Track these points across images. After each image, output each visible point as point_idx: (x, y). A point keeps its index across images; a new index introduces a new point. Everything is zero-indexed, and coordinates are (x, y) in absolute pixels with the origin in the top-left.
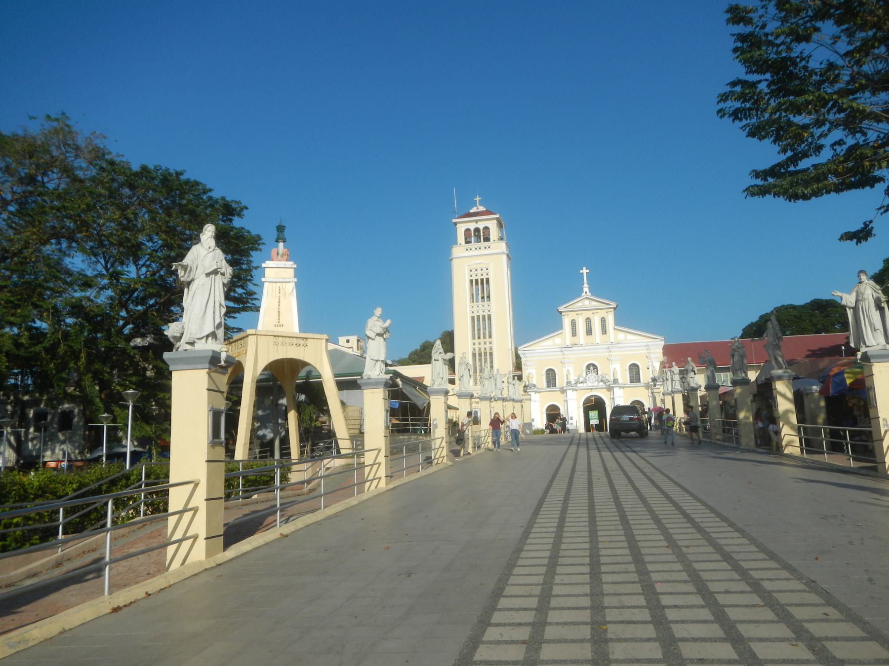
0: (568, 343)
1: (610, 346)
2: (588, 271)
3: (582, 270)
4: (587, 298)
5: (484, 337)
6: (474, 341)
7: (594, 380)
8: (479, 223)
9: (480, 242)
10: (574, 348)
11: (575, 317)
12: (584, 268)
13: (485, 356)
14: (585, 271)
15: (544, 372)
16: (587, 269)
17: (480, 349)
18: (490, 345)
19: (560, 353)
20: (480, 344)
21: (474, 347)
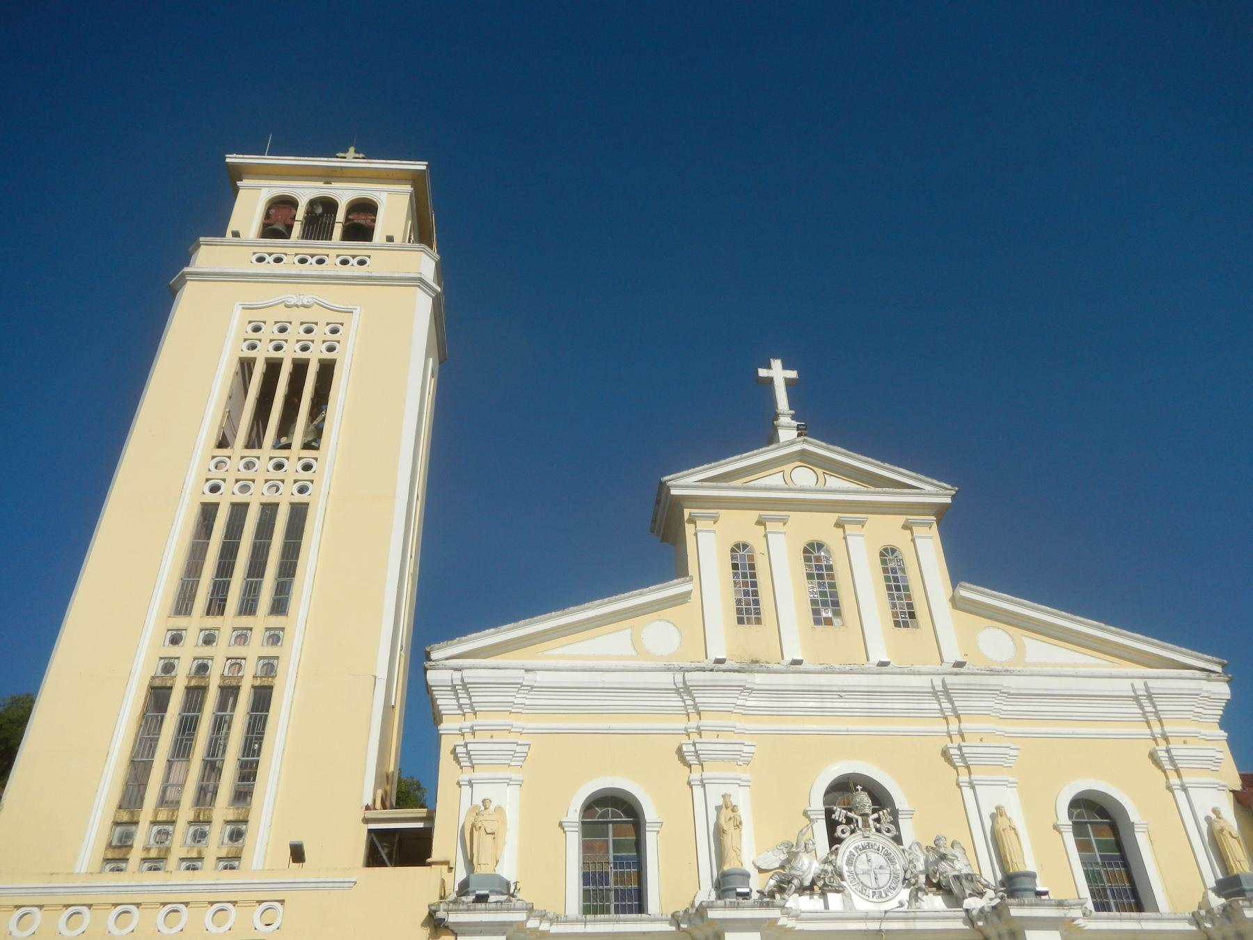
0: (717, 652)
1: (949, 679)
2: (793, 374)
3: (769, 367)
4: (805, 458)
5: (248, 607)
6: (180, 622)
7: (884, 879)
8: (334, 185)
9: (329, 237)
10: (759, 679)
11: (753, 536)
12: (777, 364)
13: (222, 706)
14: (778, 373)
15: (574, 815)
16: (785, 367)
17: (202, 669)
18: (270, 651)
19: (675, 701)
20: (209, 640)
21: (172, 651)
